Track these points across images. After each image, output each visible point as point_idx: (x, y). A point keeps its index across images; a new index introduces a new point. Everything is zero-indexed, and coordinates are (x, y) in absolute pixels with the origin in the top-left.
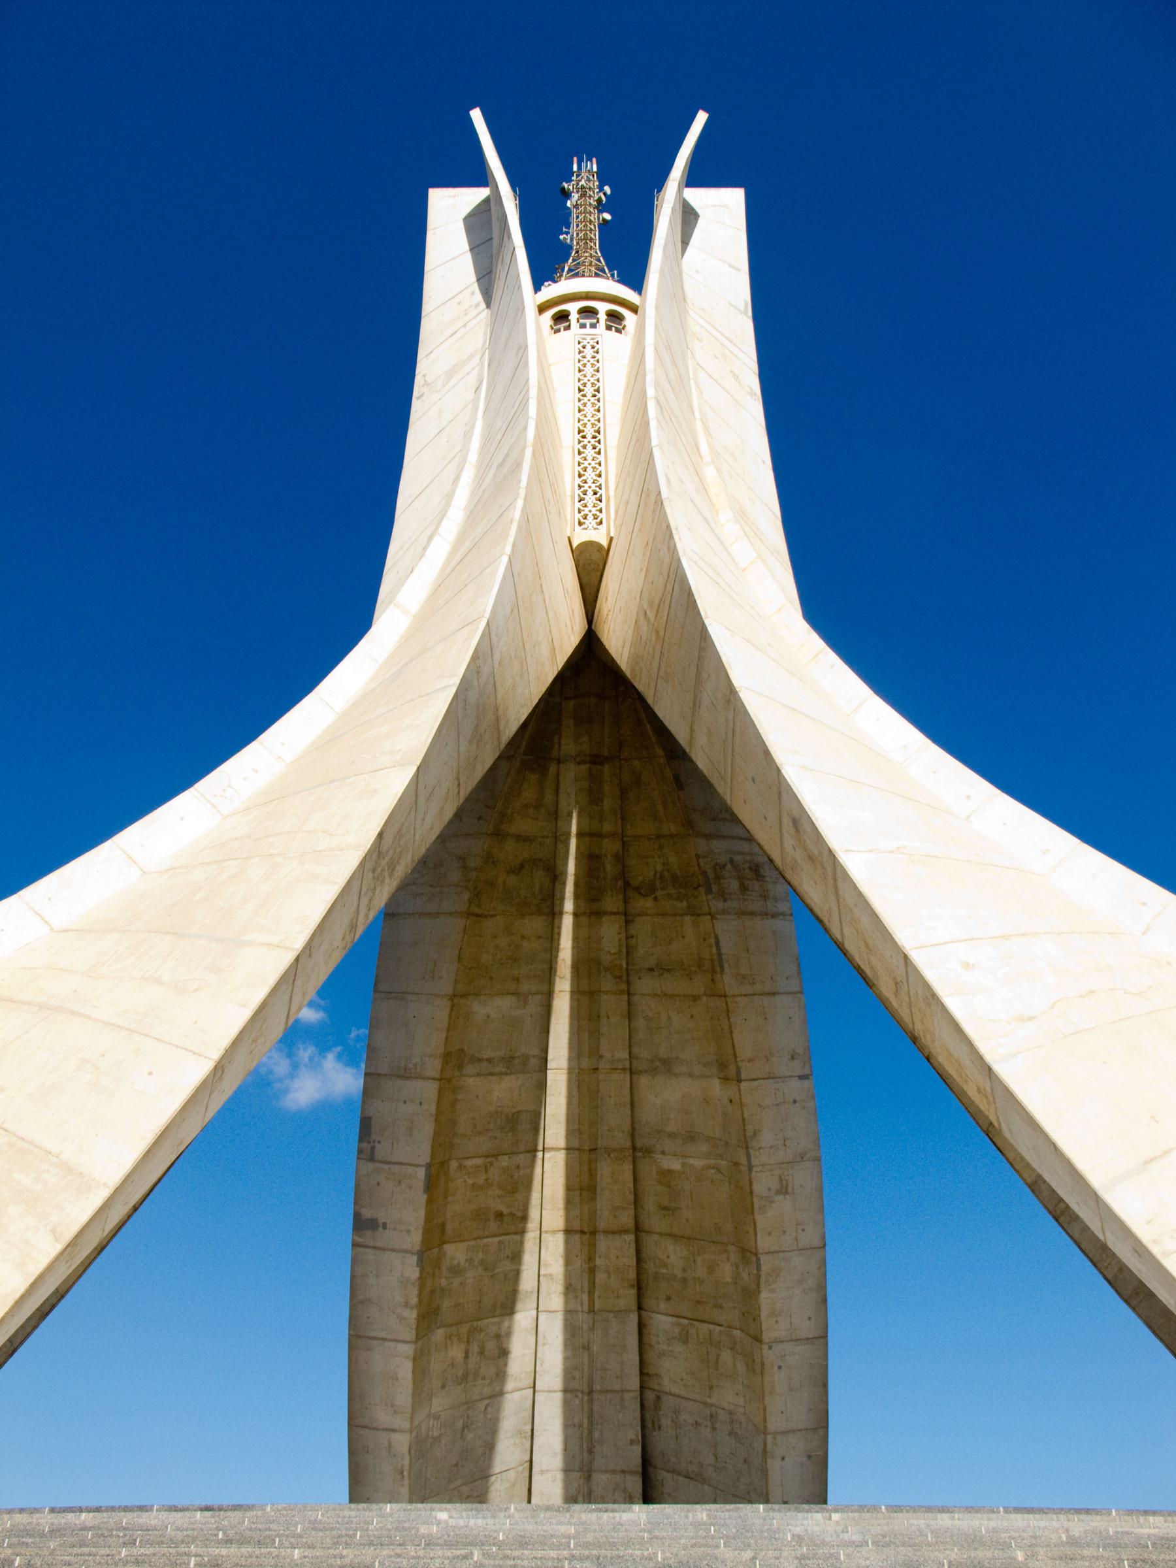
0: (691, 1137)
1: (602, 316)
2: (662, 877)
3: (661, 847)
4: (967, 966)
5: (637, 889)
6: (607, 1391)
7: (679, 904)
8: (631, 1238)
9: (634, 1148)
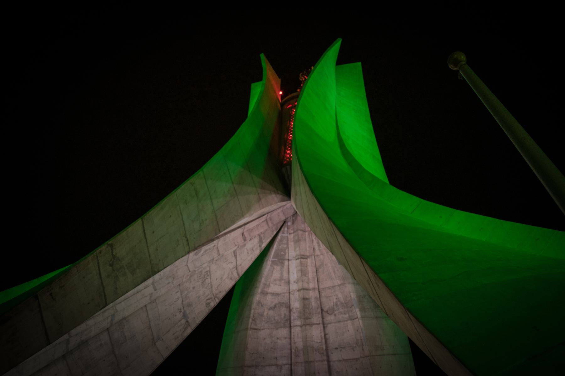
2: (336, 305)
3: (334, 291)
7: (344, 316)
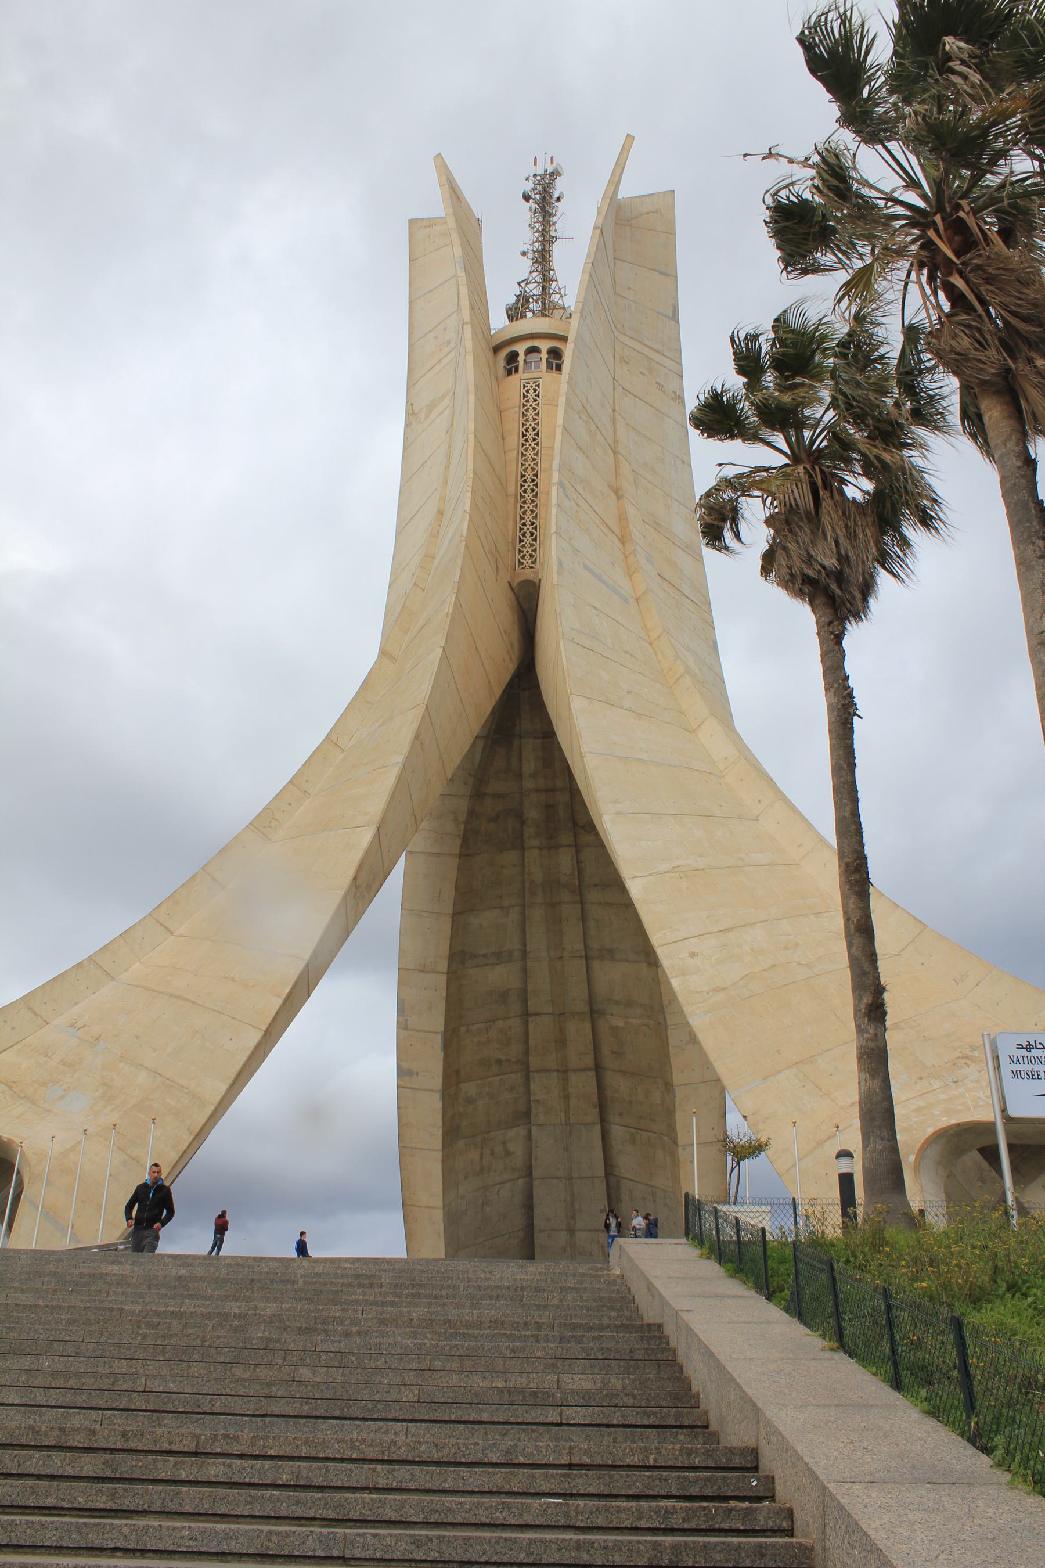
0: (629, 1004)
1: (544, 355)
4: (693, 955)
5: (583, 827)
6: (582, 1178)
8: (593, 1074)
9: (592, 1011)
